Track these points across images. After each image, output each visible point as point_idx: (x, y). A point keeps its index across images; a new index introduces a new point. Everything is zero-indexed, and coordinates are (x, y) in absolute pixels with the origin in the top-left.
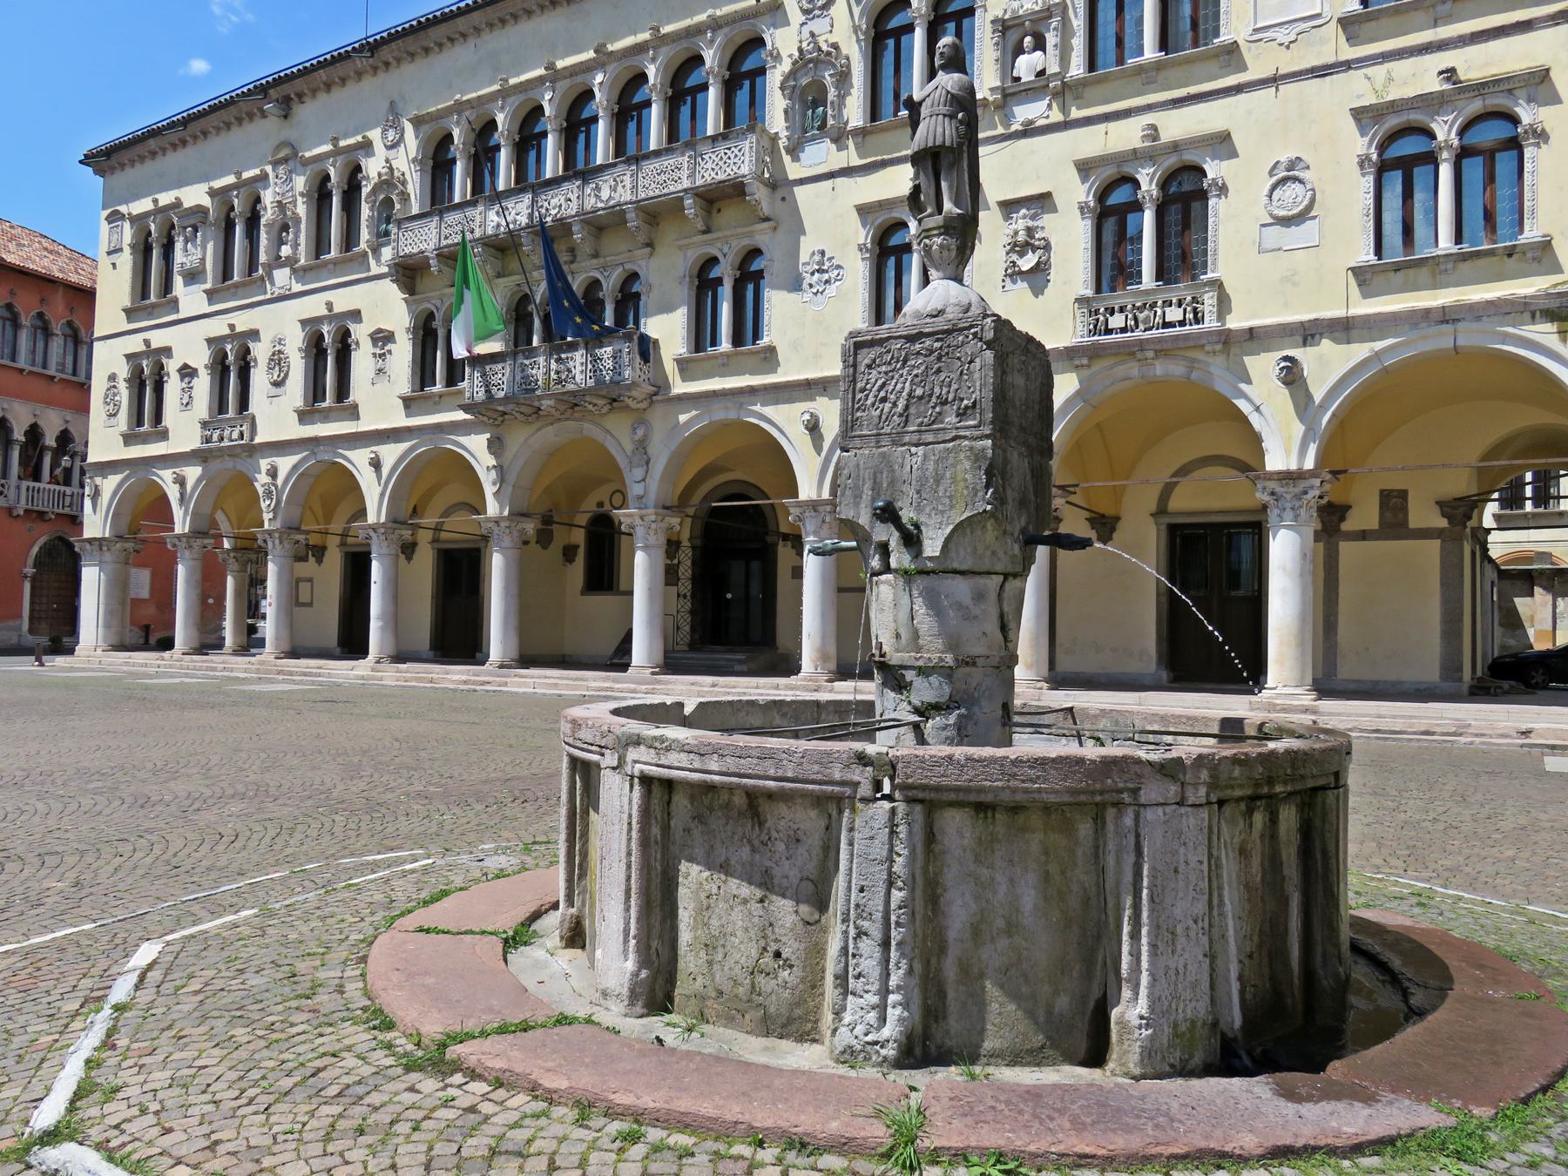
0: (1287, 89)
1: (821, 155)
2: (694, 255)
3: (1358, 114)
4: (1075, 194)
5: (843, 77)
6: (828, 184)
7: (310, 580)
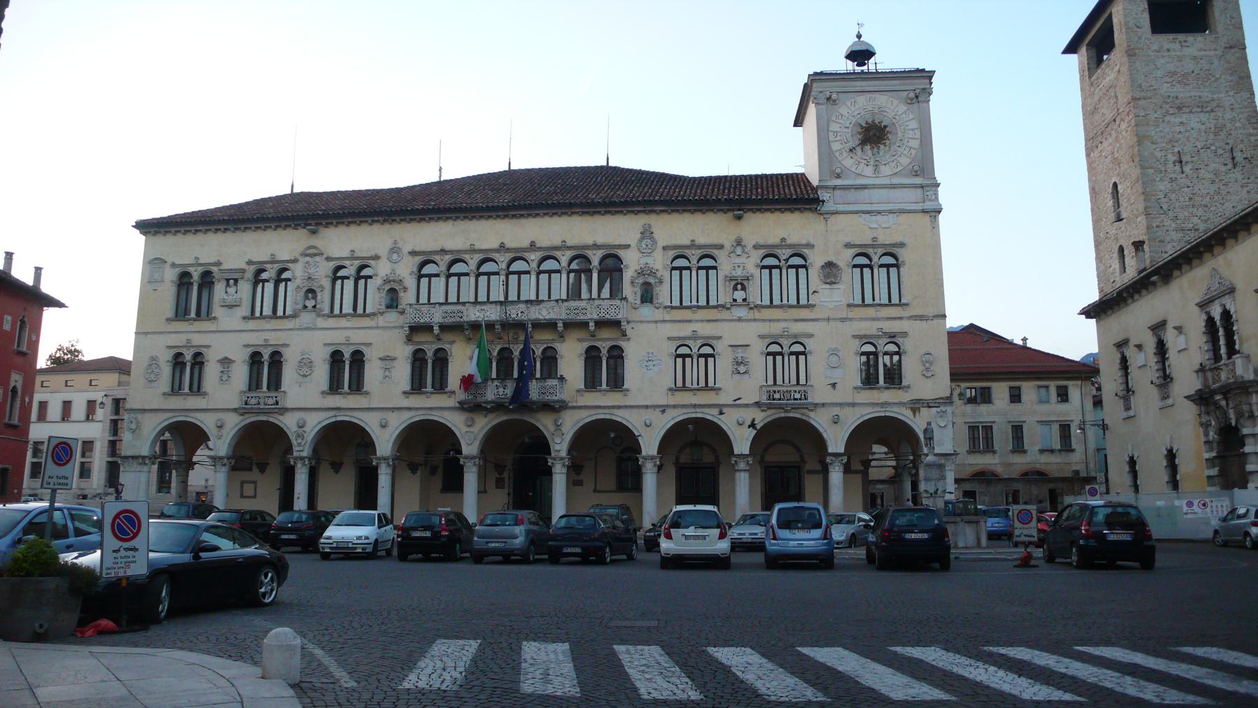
0: (832, 323)
1: (646, 311)
2: (586, 345)
3: (855, 337)
4: (758, 346)
5: (661, 282)
6: (653, 325)
7: (255, 482)
